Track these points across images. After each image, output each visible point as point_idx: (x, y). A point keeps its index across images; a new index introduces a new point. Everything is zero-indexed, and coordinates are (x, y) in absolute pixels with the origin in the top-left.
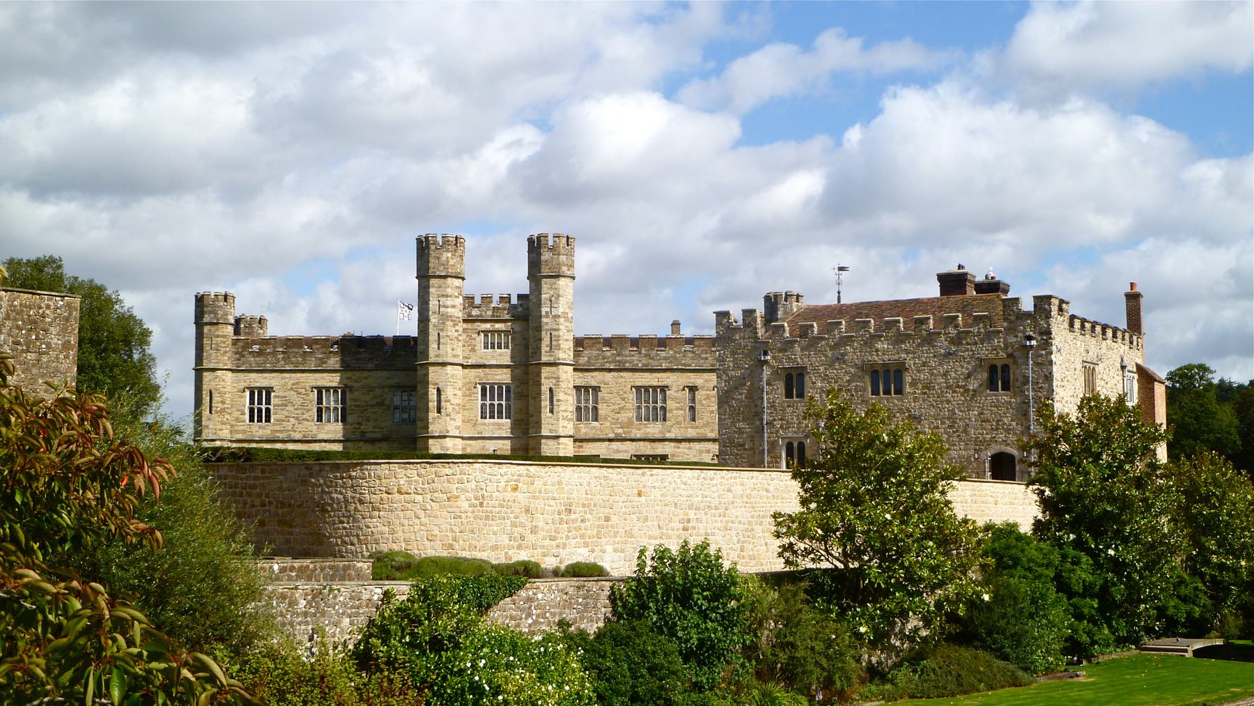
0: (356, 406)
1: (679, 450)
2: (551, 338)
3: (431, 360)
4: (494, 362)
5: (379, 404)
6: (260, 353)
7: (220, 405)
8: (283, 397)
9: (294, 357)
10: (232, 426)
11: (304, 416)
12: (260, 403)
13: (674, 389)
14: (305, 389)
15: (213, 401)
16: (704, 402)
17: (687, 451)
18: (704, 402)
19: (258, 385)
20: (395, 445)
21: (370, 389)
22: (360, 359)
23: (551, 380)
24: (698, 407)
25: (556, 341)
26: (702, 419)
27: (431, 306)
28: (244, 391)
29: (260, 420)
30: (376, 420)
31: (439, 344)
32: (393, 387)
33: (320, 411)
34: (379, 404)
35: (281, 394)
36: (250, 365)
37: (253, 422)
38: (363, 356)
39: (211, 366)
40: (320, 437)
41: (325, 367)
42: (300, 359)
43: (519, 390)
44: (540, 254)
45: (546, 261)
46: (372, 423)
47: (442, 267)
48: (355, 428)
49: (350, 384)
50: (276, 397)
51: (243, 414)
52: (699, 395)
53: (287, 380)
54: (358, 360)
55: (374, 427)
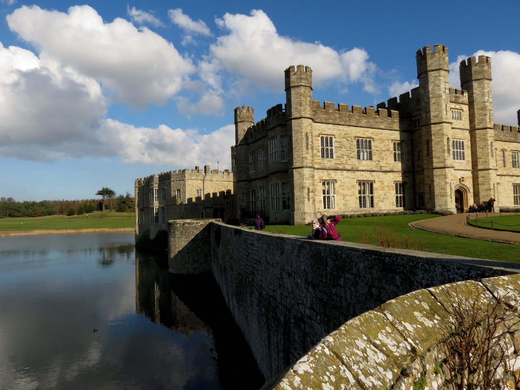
0: (377, 150)
1: (501, 181)
2: (490, 116)
3: (445, 120)
4: (456, 127)
5: (388, 150)
6: (327, 113)
9: (345, 117)
12: (327, 145)
13: (498, 150)
15: (309, 141)
16: (508, 158)
17: (504, 181)
18: (508, 158)
19: (325, 133)
20: (396, 175)
21: (383, 141)
22: (377, 122)
23: (491, 138)
24: (506, 160)
25: (492, 116)
26: (508, 166)
27: (442, 88)
30: (386, 159)
31: (446, 111)
33: (359, 152)
34: (388, 150)
35: (338, 140)
36: (321, 119)
37: (324, 157)
38: (378, 120)
41: (360, 125)
42: (347, 119)
43: (467, 144)
44: (483, 66)
45: (486, 71)
46: (385, 161)
47: (445, 66)
48: (377, 164)
49: (373, 137)
50: (336, 142)
52: (506, 153)
53: (341, 132)
54: (375, 122)
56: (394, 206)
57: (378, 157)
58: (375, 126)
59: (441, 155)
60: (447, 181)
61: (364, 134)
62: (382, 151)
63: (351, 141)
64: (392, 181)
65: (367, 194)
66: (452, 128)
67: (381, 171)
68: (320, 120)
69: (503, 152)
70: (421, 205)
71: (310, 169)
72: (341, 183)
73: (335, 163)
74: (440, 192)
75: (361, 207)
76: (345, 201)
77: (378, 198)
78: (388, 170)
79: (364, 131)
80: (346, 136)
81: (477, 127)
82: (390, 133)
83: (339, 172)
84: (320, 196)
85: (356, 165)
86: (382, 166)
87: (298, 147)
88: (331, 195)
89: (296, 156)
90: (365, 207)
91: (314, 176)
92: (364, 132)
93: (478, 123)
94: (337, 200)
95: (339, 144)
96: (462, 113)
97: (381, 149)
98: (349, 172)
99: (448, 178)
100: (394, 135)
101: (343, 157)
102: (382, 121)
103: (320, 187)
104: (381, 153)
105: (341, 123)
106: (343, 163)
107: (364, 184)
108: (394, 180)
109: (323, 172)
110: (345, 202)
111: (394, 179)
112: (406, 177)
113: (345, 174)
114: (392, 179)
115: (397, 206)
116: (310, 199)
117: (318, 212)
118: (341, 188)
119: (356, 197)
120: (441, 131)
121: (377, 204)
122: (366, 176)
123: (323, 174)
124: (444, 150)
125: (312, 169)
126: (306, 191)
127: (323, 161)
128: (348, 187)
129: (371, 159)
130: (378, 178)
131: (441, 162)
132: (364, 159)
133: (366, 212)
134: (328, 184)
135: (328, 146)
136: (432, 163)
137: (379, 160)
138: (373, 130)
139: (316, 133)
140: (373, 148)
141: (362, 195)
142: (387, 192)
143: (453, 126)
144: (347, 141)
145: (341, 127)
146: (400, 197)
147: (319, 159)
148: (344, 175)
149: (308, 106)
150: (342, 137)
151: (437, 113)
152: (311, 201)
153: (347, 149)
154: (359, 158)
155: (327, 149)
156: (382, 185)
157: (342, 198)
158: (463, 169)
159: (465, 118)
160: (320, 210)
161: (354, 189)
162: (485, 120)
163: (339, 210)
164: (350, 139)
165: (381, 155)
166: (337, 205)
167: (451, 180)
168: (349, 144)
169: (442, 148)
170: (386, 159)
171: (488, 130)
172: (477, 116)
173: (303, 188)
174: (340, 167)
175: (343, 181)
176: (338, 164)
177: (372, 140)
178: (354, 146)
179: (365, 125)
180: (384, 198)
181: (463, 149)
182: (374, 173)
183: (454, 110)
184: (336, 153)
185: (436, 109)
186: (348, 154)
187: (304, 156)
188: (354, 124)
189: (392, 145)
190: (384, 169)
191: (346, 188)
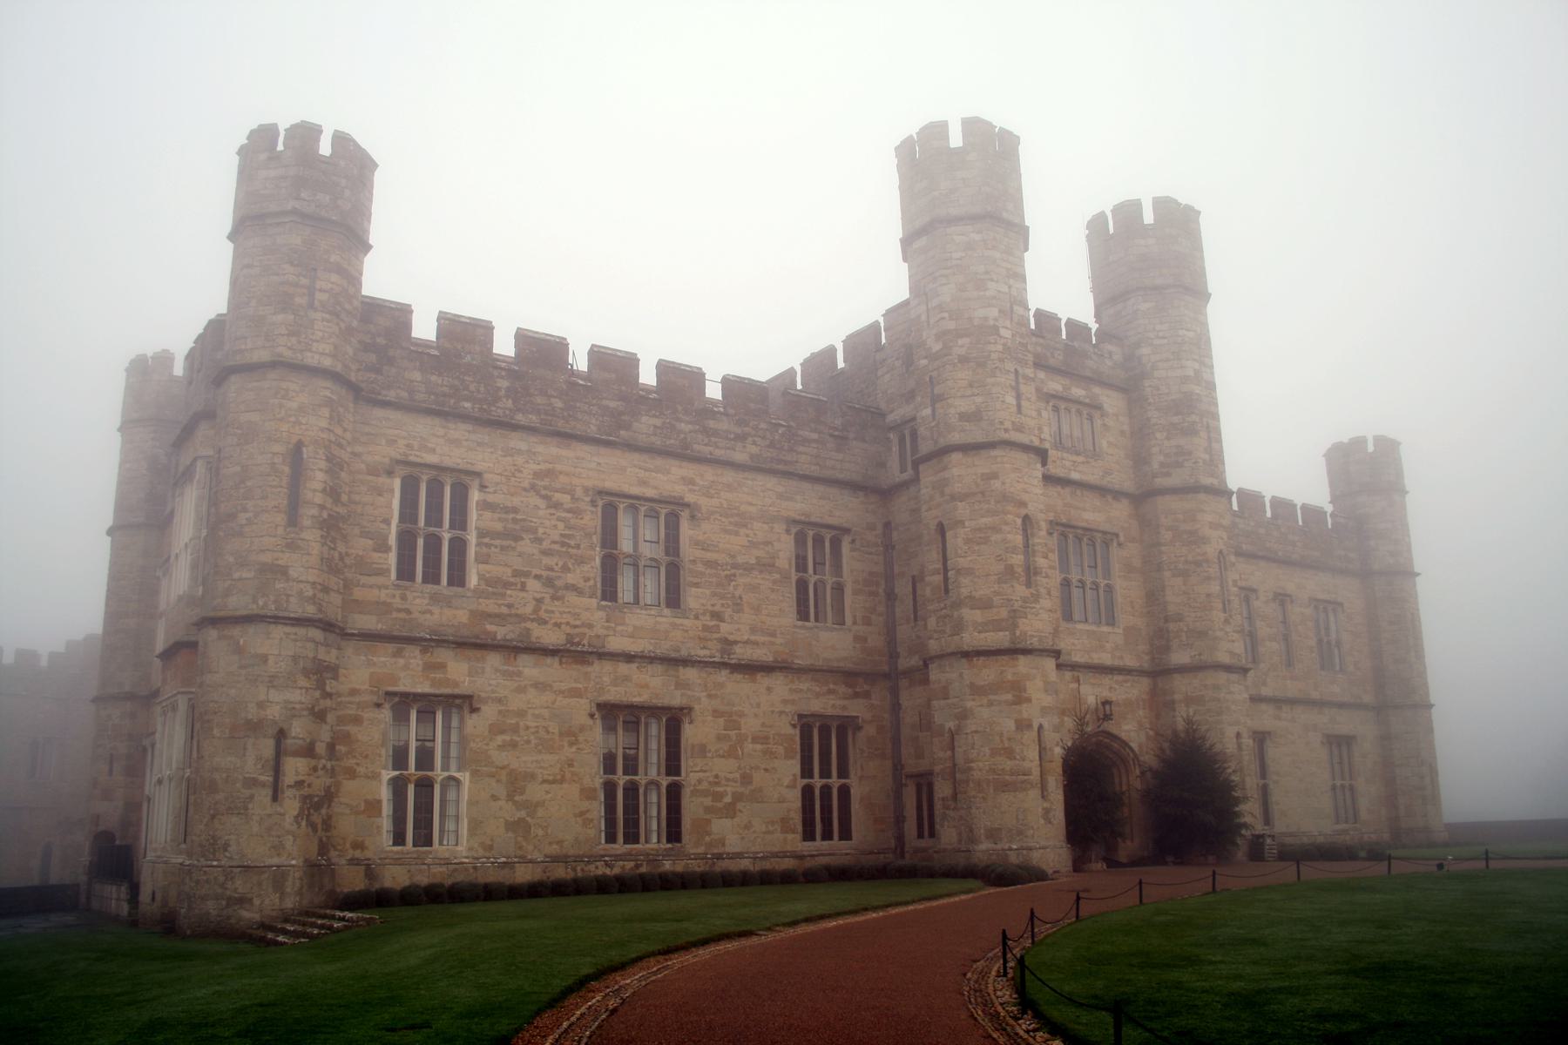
0: (709, 564)
5: (766, 566)
7: (329, 503)
8: (507, 510)
10: (348, 585)
11: (571, 578)
12: (434, 517)
14: (571, 492)
20: (804, 686)
22: (716, 433)
28: (390, 473)
29: (432, 577)
30: (757, 610)
31: (1018, 397)
32: (795, 522)
33: (610, 566)
39: (311, 359)
40: (616, 644)
42: (558, 404)
48: (706, 628)
51: (383, 547)
53: (520, 460)
54: (706, 431)
55: (753, 630)
56: (790, 836)
57: (714, 594)
58: (702, 449)
59: (997, 593)
60: (1025, 715)
61: (643, 483)
62: (735, 566)
63: (569, 511)
64: (781, 713)
65: (652, 770)
66: (1048, 479)
67: (724, 665)
68: (405, 394)
69: (1282, 604)
70: (926, 833)
71: (301, 631)
72: (500, 712)
73: (473, 613)
74: (993, 771)
75: (611, 838)
76: (517, 804)
77: (705, 793)
78: (765, 659)
79: (646, 470)
80: (546, 482)
81: (1161, 482)
82: (780, 489)
83: (494, 660)
84: (376, 776)
85: (590, 626)
86: (731, 638)
87: (245, 510)
88: (439, 774)
89: (231, 559)
90: (633, 837)
91: (333, 670)
92: (642, 474)
93: (1162, 465)
94: (471, 803)
95: (500, 519)
96: (1098, 422)
97: (733, 557)
98: (549, 660)
99: (1029, 700)
100: (798, 498)
101: (523, 588)
102: (739, 430)
103: (376, 729)
104: (731, 578)
105: (520, 418)
106: (517, 615)
107: (633, 725)
108: (789, 708)
109: (398, 654)
110: (523, 814)
111: (793, 702)
112: (856, 695)
113: (527, 671)
114: (785, 702)
115: (809, 835)
116: (289, 793)
117: (354, 862)
118: (500, 739)
119: (582, 790)
120: (996, 484)
121: (702, 826)
122: (646, 686)
123: (401, 661)
124: (1010, 570)
125: (317, 634)
126: (267, 747)
127: (403, 598)
128: (542, 733)
129: (673, 599)
130: (709, 696)
131: (996, 625)
132: (637, 601)
133: (637, 866)
134: (426, 715)
135: (440, 524)
136: (959, 627)
137: (717, 608)
138: (688, 470)
139: (382, 453)
140: (687, 551)
141: (621, 779)
142: (757, 768)
143: (1055, 469)
144: (549, 507)
145: (518, 441)
146: (826, 790)
147: (379, 588)
148: (519, 674)
149: (318, 315)
150: (526, 484)
151: (979, 400)
152: (291, 805)
153: (546, 545)
154: (609, 592)
155: (439, 540)
156: (732, 733)
157: (502, 792)
158: (1106, 659)
159: (1110, 443)
160: (368, 854)
161: (574, 749)
162: (1190, 453)
163: (481, 852)
164: (565, 499)
165: (731, 588)
166: (473, 831)
167: (1045, 711)
168: (561, 525)
169: (999, 559)
170: (757, 610)
171: (1202, 496)
172: (1158, 435)
173: (255, 727)
174: (501, 632)
175: (517, 703)
176: (490, 615)
177: (685, 514)
178: (589, 535)
179: (653, 439)
180: (738, 797)
181: (1107, 573)
182: (690, 674)
183: (1062, 406)
184: (482, 559)
185: (971, 386)
186: (551, 569)
187: (267, 558)
188: (592, 430)
189: (785, 549)
190: (742, 653)
191: (528, 742)
